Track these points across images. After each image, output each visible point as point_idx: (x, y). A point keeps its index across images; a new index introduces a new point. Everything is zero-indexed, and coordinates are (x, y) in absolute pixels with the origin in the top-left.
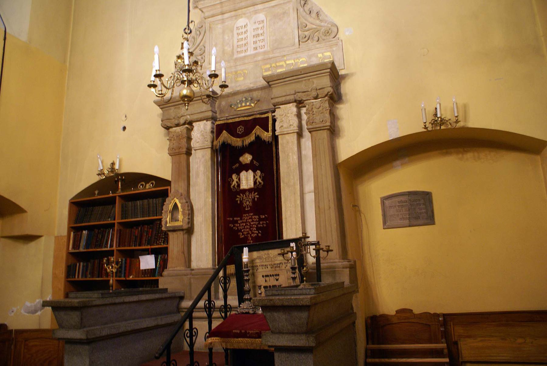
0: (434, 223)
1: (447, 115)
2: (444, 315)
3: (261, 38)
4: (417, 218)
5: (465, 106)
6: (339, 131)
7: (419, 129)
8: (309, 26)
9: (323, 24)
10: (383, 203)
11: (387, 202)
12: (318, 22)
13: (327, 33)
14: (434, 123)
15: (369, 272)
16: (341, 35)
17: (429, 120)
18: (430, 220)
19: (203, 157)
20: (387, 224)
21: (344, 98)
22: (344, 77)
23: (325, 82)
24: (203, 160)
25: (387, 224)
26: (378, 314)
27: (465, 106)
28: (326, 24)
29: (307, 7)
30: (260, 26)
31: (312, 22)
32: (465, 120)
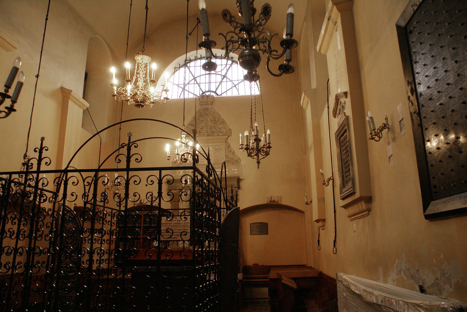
0: (268, 234)
1: (275, 199)
2: (269, 266)
5: (281, 196)
7: (266, 203)
9: (235, 157)
10: (251, 226)
13: (237, 161)
14: (271, 201)
17: (269, 201)
18: (266, 232)
19: (186, 204)
20: (251, 234)
22: (241, 180)
23: (235, 183)
24: (186, 205)
25: (251, 234)
27: (281, 196)
29: (229, 149)
31: (231, 156)
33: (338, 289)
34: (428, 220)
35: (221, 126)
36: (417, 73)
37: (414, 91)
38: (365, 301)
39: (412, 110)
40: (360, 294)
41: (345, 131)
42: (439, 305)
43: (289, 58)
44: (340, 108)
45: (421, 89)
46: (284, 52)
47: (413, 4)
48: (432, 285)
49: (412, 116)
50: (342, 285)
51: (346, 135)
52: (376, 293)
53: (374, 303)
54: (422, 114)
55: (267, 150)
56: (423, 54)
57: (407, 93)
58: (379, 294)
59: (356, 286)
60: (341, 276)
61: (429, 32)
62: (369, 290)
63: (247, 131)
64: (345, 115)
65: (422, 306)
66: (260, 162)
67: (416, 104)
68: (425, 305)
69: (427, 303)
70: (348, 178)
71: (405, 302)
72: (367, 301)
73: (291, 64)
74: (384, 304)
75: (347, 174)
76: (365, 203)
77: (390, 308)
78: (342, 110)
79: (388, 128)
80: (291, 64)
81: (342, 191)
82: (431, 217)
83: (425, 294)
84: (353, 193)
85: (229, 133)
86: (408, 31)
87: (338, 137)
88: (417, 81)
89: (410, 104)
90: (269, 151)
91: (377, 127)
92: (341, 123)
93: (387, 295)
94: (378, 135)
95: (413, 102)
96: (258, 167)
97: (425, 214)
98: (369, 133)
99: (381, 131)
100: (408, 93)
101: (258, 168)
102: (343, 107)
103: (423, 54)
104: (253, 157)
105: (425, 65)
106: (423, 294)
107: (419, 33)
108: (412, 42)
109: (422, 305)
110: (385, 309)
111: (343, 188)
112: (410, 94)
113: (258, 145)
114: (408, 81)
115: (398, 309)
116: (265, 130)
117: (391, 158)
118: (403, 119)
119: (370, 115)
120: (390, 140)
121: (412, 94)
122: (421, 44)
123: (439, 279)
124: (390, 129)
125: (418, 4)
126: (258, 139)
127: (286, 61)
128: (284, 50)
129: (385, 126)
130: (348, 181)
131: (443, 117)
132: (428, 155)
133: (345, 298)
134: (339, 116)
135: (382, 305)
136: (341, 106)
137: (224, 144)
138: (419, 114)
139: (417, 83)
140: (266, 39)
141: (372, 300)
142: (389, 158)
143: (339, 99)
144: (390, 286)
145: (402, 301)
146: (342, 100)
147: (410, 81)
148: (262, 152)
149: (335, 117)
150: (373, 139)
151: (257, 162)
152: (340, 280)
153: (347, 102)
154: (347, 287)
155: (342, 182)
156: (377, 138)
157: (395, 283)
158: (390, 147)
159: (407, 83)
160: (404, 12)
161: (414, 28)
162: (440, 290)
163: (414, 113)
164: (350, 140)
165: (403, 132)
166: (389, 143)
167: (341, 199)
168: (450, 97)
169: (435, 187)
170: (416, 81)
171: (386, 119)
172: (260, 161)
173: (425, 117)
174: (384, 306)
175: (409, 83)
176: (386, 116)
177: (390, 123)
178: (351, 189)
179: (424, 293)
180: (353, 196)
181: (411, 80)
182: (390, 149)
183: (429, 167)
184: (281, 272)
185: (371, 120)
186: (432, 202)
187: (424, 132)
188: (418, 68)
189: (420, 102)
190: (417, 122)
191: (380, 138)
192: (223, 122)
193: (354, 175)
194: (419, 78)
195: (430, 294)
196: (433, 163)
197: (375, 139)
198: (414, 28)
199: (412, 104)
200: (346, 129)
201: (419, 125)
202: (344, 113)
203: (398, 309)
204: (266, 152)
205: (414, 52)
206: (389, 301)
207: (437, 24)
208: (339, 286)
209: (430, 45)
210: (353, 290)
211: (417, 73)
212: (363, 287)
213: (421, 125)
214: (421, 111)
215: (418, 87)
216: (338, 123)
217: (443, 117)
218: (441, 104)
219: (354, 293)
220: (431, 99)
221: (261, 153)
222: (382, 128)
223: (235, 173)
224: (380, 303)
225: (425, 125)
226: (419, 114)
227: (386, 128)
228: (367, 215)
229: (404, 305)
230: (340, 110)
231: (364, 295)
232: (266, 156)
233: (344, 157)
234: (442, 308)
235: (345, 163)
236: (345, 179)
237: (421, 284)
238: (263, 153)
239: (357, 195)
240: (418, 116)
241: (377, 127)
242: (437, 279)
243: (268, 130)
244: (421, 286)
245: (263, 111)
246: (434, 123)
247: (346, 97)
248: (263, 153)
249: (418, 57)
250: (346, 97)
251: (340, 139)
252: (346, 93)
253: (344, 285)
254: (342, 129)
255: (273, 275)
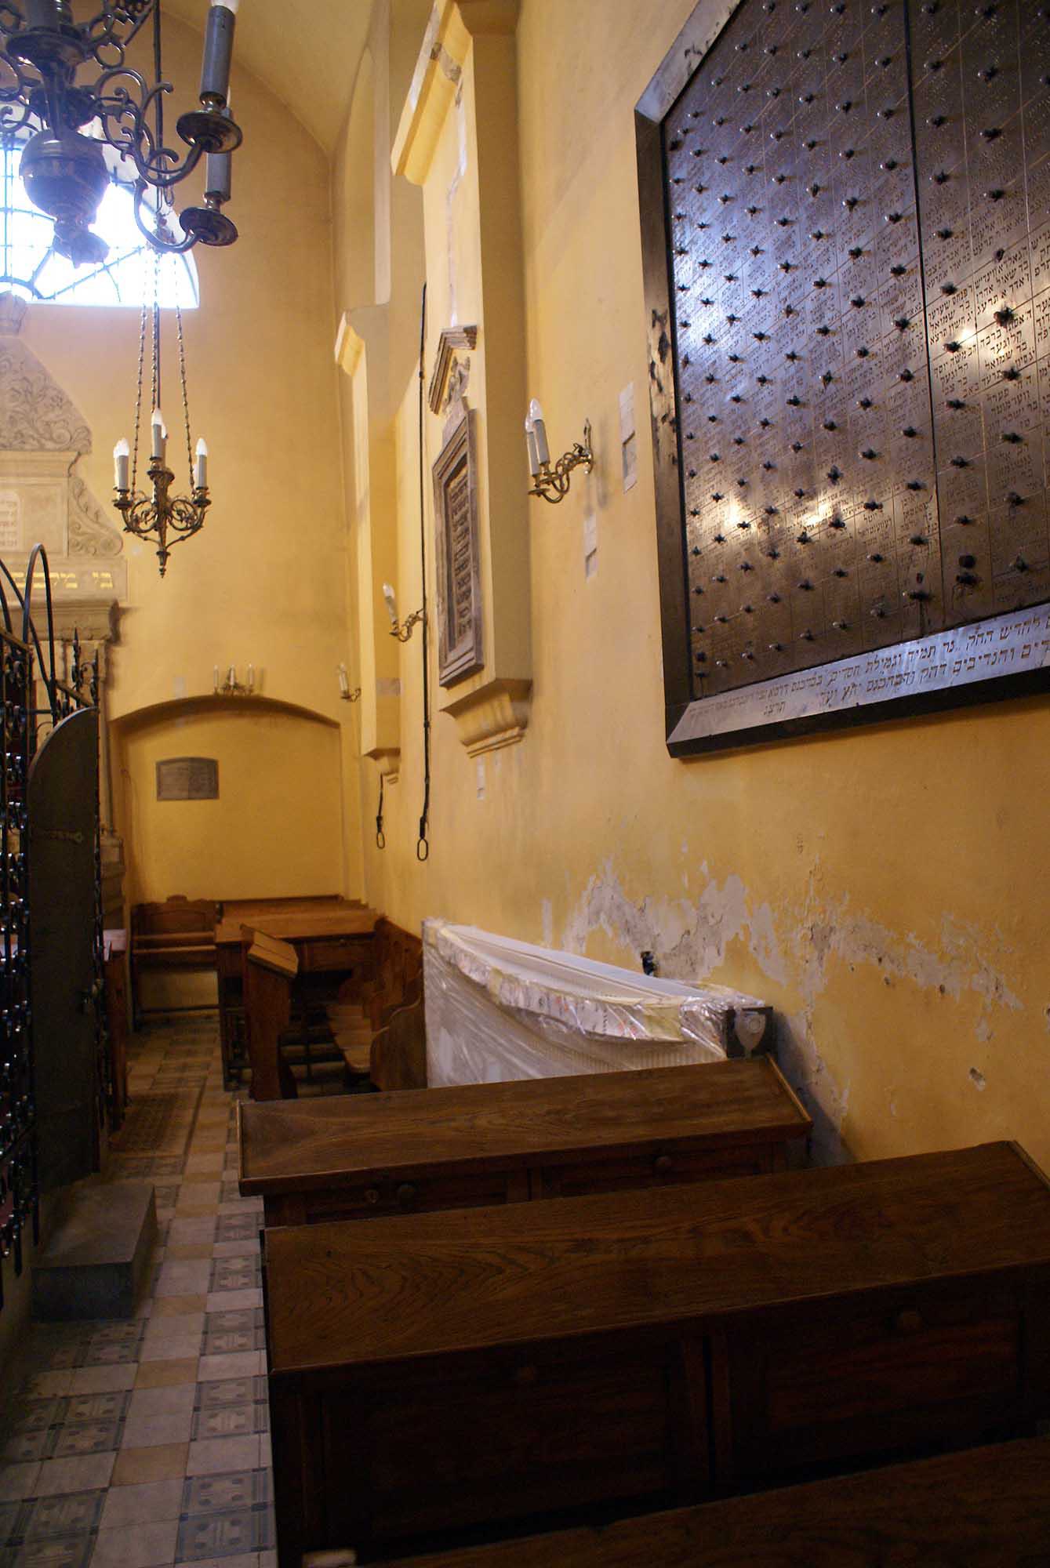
1: (242, 681)
2: (222, 903)
3: (11, 529)
4: (198, 790)
5: (263, 672)
6: (113, 680)
7: (211, 692)
8: (84, 529)
9: (103, 531)
11: (164, 769)
12: (96, 526)
13: (108, 545)
14: (227, 687)
15: (136, 852)
16: (124, 552)
17: (222, 683)
18: (213, 792)
20: (161, 795)
21: (122, 639)
22: (125, 611)
23: (103, 621)
25: (161, 795)
26: (145, 902)
28: (107, 533)
29: (83, 501)
30: (11, 510)
31: (87, 525)
32: (261, 686)
33: (427, 970)
34: (676, 760)
35: (51, 416)
36: (683, 289)
37: (668, 346)
38: (497, 1003)
39: (658, 410)
40: (483, 983)
41: (463, 463)
42: (681, 1006)
43: (218, 187)
44: (453, 380)
45: (690, 340)
46: (193, 160)
47: (688, 46)
48: (674, 949)
49: (655, 430)
50: (436, 955)
51: (466, 476)
52: (527, 977)
53: (519, 1010)
54: (684, 425)
55: (195, 511)
56: (702, 226)
57: (649, 352)
58: (535, 981)
59: (473, 959)
60: (436, 931)
61: (726, 154)
62: (510, 970)
63: (124, 440)
64: (466, 406)
65: (639, 1011)
66: (168, 554)
67: (672, 390)
68: (649, 1007)
69: (653, 1001)
70: (466, 619)
71: (598, 1001)
72: (501, 1003)
73: (225, 209)
74: (545, 1011)
75: (464, 605)
76: (512, 700)
77: (557, 1020)
78: (458, 387)
79: (589, 461)
80: (225, 209)
81: (446, 658)
82: (686, 751)
83: (655, 976)
84: (476, 669)
85: (80, 445)
86: (670, 139)
87: (440, 478)
88: (680, 315)
89: (655, 388)
90: (203, 514)
91: (555, 456)
92: (453, 431)
93: (555, 985)
94: (557, 483)
95: (663, 383)
96: (163, 571)
97: (670, 741)
98: (531, 473)
99: (567, 470)
100: (652, 351)
101: (163, 574)
102: (462, 378)
103: (702, 226)
104: (143, 535)
105: (705, 264)
106: (651, 978)
107: (698, 153)
108: (677, 181)
109: (640, 1007)
110: (548, 1023)
111: (450, 650)
112: (656, 356)
113: (161, 492)
114: (654, 312)
115: (579, 1022)
116: (189, 439)
117: (593, 559)
118: (633, 435)
119: (535, 412)
120: (595, 503)
121: (662, 359)
122: (700, 190)
123: (692, 932)
124: (595, 466)
125: (704, 50)
126: (162, 473)
127: (208, 195)
128: (189, 156)
129: (580, 455)
130: (464, 626)
131: (739, 442)
132: (691, 558)
133: (444, 995)
134: (448, 409)
135: (539, 1015)
136: (457, 376)
137: (64, 481)
138: (677, 424)
139: (678, 322)
140: (129, 101)
141: (516, 1001)
142: (588, 558)
143: (452, 349)
144: (571, 958)
145: (590, 1000)
146: (461, 353)
147: (660, 313)
148: (179, 518)
149: (436, 411)
150: (541, 493)
151: (158, 553)
152: (431, 940)
153: (474, 360)
154: (449, 963)
155: (447, 632)
156: (553, 494)
157: (584, 948)
158: (593, 523)
159: (650, 319)
160: (664, 68)
161: (686, 132)
162: (692, 964)
163: (664, 419)
164: (475, 492)
165: (630, 479)
166: (589, 511)
167: (442, 685)
168: (763, 380)
169: (702, 658)
170: (678, 314)
171: (587, 431)
172: (168, 550)
173: (691, 437)
174: (548, 1017)
175: (656, 318)
176: (587, 421)
177: (596, 448)
178: (472, 655)
179: (652, 973)
180: (477, 678)
181: (662, 308)
182: (591, 533)
183: (692, 596)
184: (254, 920)
185: (538, 430)
186: (692, 705)
187: (686, 483)
188: (684, 270)
189: (682, 385)
190: (668, 448)
191: (563, 491)
192: (60, 401)
193: (480, 610)
194: (687, 304)
195: (667, 976)
196: (702, 583)
197: (547, 494)
198: (686, 132)
199: (661, 389)
200: (465, 456)
201: (674, 460)
202: (464, 399)
203: (579, 1022)
204: (189, 519)
205: (679, 217)
206: (558, 1000)
207: (748, 130)
208: (429, 961)
209: (725, 199)
210: (466, 971)
211: (683, 289)
212: (493, 963)
213: (678, 461)
214: (684, 416)
215: (681, 336)
216: (444, 432)
217: (739, 442)
218: (737, 399)
219: (468, 981)
220: (711, 379)
221: (174, 521)
222: (571, 461)
223: (103, 585)
224: (534, 1007)
225: (690, 463)
226: (677, 424)
227: (584, 461)
228: (517, 739)
229: (597, 1010)
230: (452, 388)
231: (495, 985)
232: (189, 531)
233: (457, 547)
234: (686, 1013)
235: (459, 568)
236: (457, 620)
237: (647, 949)
238: (182, 521)
239: (488, 676)
240: (674, 431)
241: (555, 456)
242: (688, 932)
243: (201, 440)
244: (648, 953)
245: (183, 373)
246: (715, 459)
247: (473, 344)
248: (182, 521)
249: (688, 234)
250: (473, 344)
251: (447, 485)
252: (471, 332)
253: (442, 958)
254: (455, 454)
255: (227, 931)
